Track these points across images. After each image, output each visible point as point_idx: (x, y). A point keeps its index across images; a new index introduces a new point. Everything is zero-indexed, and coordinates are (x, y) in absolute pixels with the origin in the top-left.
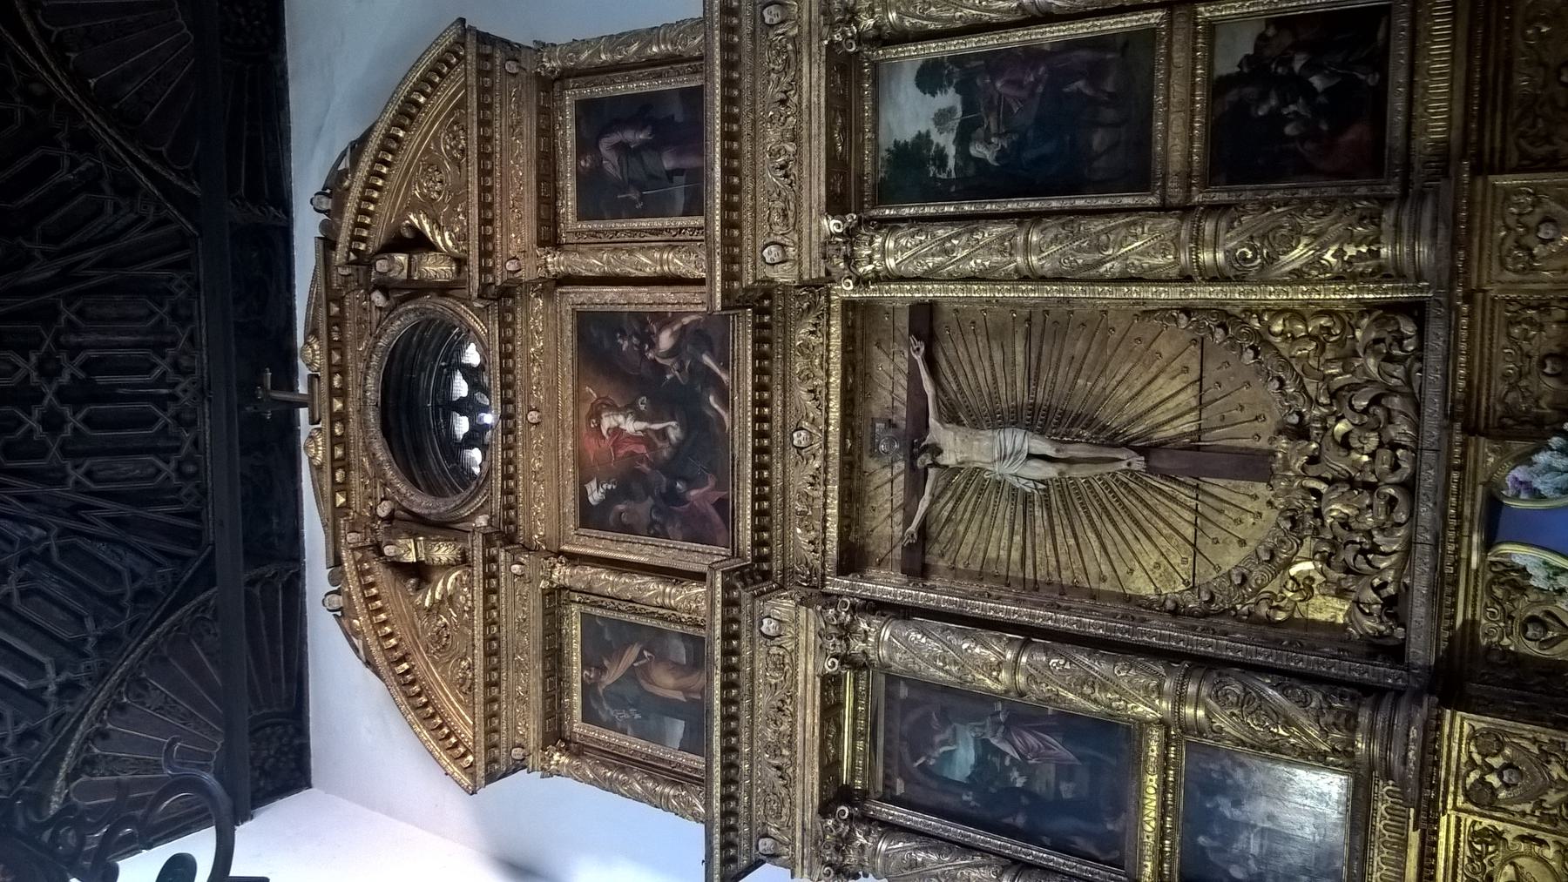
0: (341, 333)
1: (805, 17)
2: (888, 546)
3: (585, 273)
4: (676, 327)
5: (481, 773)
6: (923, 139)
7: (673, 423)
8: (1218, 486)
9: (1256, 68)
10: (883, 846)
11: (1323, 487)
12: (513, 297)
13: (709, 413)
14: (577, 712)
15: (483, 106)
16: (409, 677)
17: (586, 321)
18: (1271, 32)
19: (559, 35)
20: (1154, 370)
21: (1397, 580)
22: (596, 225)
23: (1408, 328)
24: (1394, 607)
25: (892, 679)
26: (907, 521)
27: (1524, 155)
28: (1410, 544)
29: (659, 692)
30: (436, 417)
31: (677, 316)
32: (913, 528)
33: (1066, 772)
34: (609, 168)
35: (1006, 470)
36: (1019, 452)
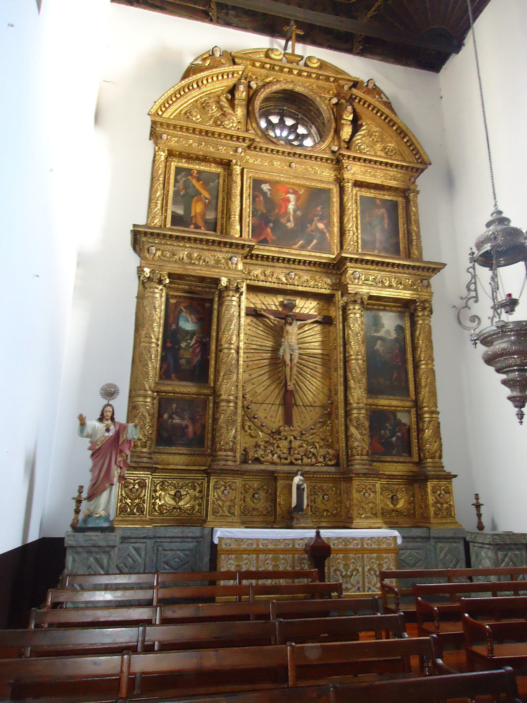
0: (322, 80)
1: (424, 294)
2: (253, 302)
3: (345, 198)
4: (325, 231)
5: (157, 119)
6: (382, 326)
7: (293, 225)
8: (281, 410)
9: (398, 423)
10: (157, 295)
11: (289, 440)
12: (335, 164)
13: (297, 240)
14: (180, 165)
15: (402, 167)
16: (191, 88)
18: (407, 427)
19: (421, 199)
20: (315, 393)
21: (265, 462)
23: (333, 462)
24: (257, 460)
25: (211, 301)
30: (280, 109)
32: (263, 313)
33: (189, 361)
36: (293, 351)
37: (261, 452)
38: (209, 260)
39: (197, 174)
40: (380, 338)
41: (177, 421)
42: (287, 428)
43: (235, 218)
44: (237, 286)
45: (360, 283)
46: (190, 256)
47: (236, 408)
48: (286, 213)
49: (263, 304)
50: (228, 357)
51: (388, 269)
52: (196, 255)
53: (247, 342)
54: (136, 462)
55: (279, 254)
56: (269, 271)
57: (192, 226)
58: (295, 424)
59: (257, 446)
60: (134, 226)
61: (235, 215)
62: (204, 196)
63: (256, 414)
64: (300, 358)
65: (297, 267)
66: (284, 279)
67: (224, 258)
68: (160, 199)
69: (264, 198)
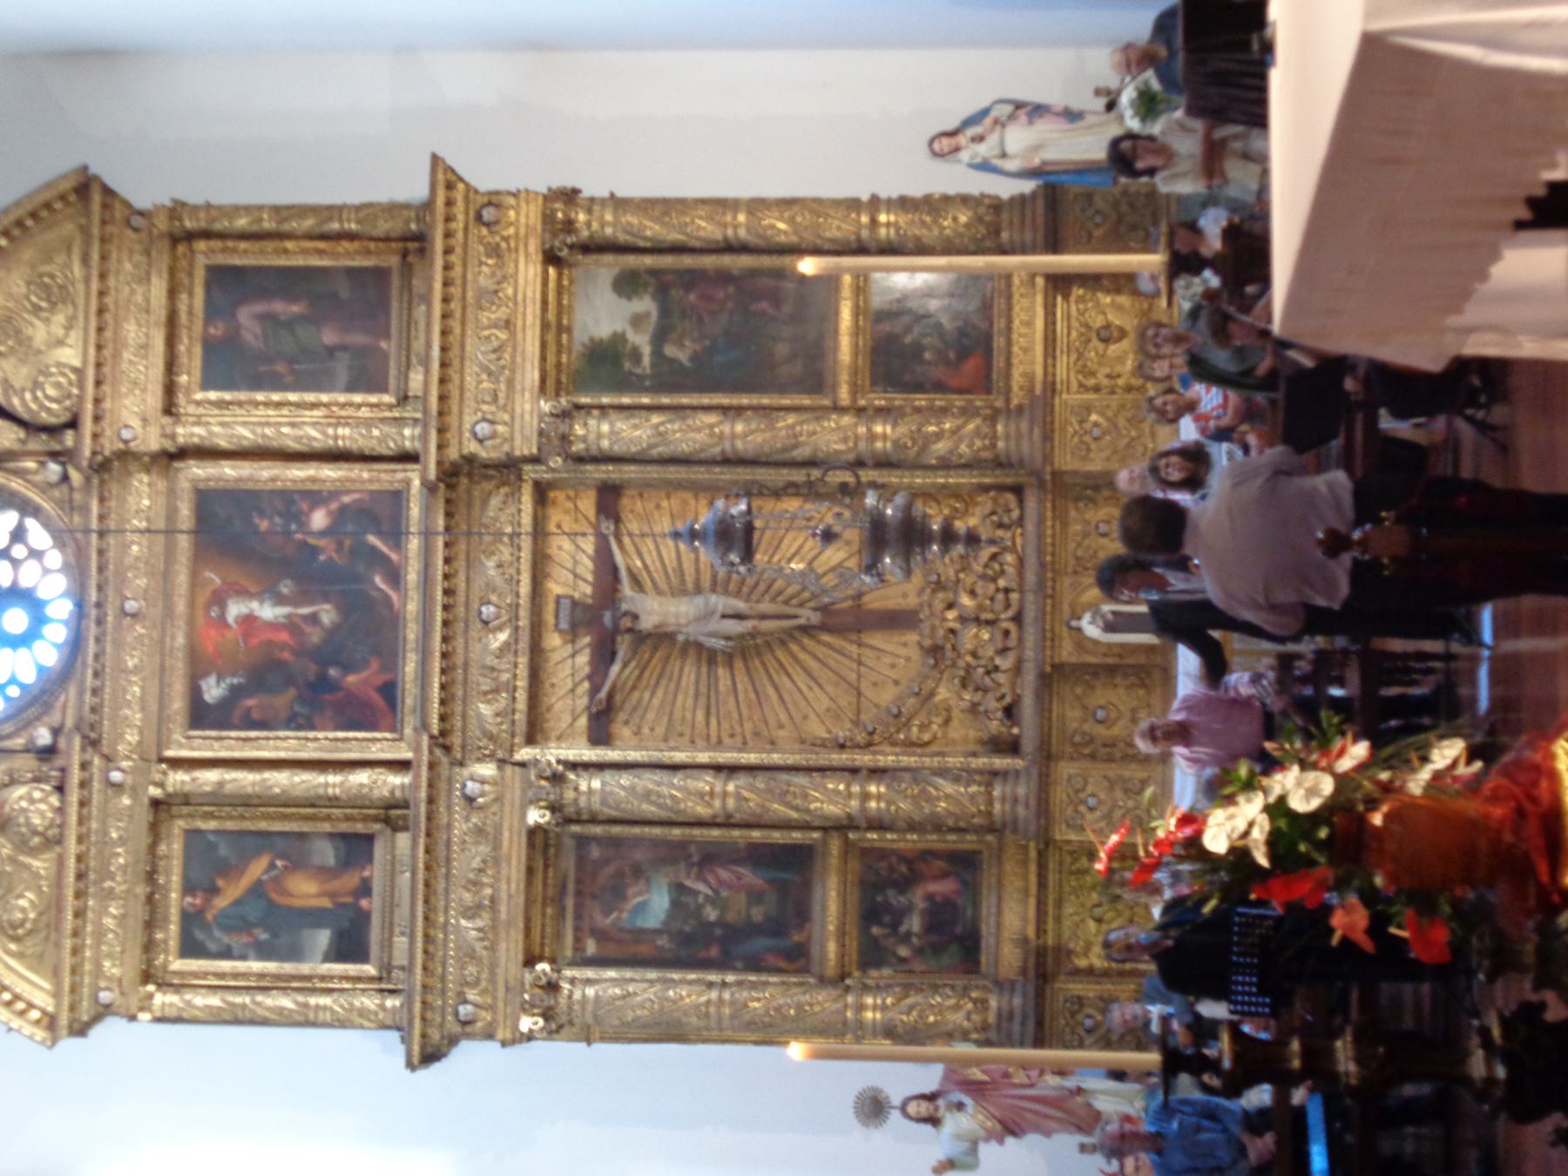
1: (523, 220)
2: (569, 720)
3: (223, 444)
4: (334, 506)
6: (619, 338)
7: (327, 607)
8: (876, 639)
10: (590, 992)
13: (374, 594)
14: (173, 944)
15: (104, 258)
17: (206, 499)
21: (1013, 690)
22: (227, 396)
24: (1010, 712)
25: (582, 841)
26: (594, 690)
27: (1081, 385)
28: (1019, 664)
29: (297, 903)
31: (335, 495)
32: (603, 694)
33: (756, 897)
34: (248, 337)
35: (693, 632)
36: (713, 613)
37: (992, 704)
38: (478, 859)
39: (194, 896)
40: (660, 338)
41: (914, 923)
42: (926, 627)
43: (334, 786)
44: (546, 779)
45: (506, 417)
46: (471, 912)
47: (877, 773)
48: (291, 625)
49: (572, 691)
50: (747, 800)
51: (457, 331)
52: (467, 896)
53: (687, 738)
54: (1023, 1024)
55: (431, 654)
56: (481, 679)
57: (364, 903)
58: (912, 601)
59: (974, 707)
60: (411, 1065)
61: (327, 785)
62: (267, 871)
63: (888, 710)
64: (738, 594)
65: (461, 597)
66: (503, 636)
67: (467, 819)
68: (301, 998)
69: (250, 696)
